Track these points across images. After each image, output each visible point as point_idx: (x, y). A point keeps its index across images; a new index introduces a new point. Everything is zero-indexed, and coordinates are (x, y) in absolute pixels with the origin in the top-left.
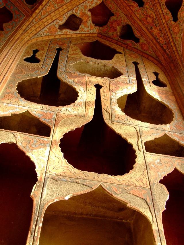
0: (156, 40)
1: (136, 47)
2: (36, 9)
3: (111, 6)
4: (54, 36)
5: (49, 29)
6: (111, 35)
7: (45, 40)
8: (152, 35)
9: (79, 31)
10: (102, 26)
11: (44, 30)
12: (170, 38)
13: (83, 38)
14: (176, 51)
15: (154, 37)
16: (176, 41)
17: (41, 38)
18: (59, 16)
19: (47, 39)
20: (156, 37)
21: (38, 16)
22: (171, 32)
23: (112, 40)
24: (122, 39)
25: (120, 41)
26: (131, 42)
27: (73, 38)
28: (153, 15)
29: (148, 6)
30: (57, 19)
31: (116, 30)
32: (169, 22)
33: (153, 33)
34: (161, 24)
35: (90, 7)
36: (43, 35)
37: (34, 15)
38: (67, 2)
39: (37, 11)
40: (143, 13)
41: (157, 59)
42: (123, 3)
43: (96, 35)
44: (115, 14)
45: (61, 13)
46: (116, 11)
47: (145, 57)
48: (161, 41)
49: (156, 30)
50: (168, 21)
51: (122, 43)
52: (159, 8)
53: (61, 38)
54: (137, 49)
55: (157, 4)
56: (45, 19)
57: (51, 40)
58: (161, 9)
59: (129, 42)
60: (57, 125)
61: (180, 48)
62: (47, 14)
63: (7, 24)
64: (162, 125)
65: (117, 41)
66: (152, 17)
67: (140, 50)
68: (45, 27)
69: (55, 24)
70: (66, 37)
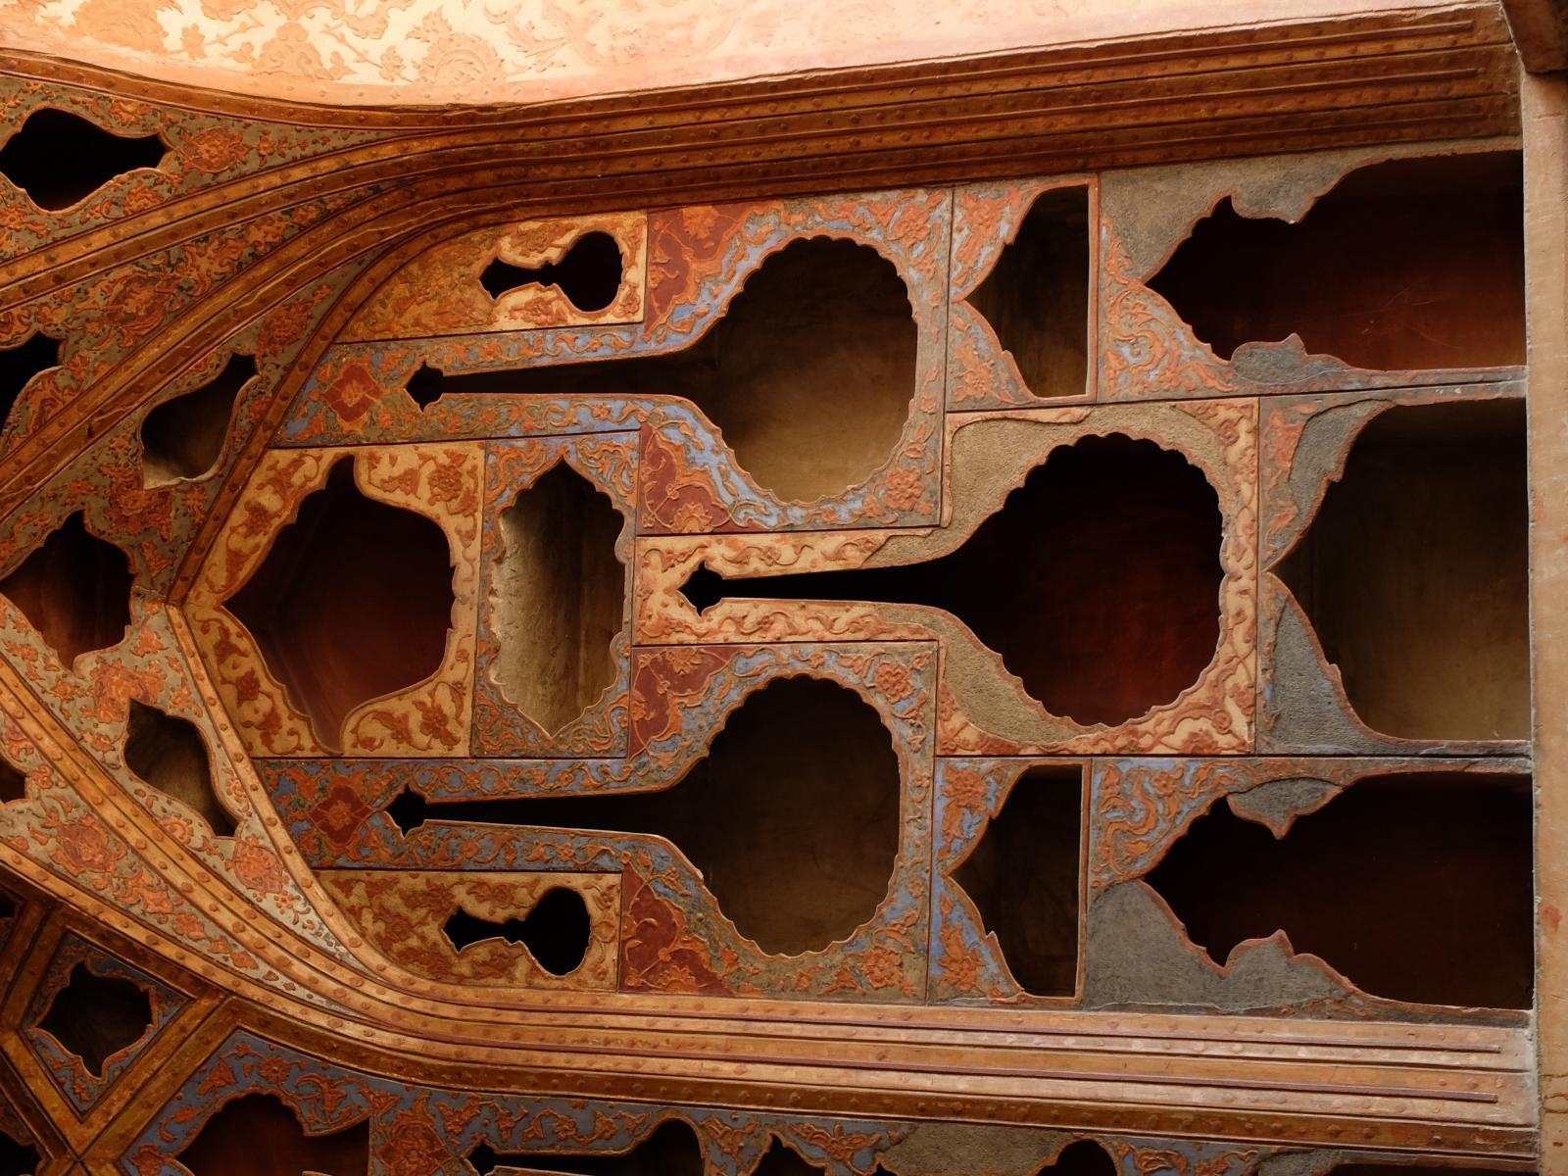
0: (257, 259)
1: (275, 379)
2: (178, 970)
3: (30, 532)
4: (287, 857)
5: (262, 884)
6: (186, 521)
7: (335, 901)
8: (225, 282)
9: (200, 716)
10: (130, 579)
11: (282, 913)
12: (262, 183)
13: (229, 692)
14: (346, 157)
15: (240, 269)
16: (283, 155)
17: (330, 921)
18: (168, 840)
19: (317, 888)
20: (240, 264)
21: (218, 957)
22: (222, 178)
23: (216, 519)
24: (221, 457)
25: (226, 470)
26: (245, 407)
27: (248, 747)
28: (114, 282)
29: (60, 316)
30: (187, 851)
31: (164, 494)
32: (163, 190)
33: (213, 281)
34: (173, 235)
35: (54, 661)
36: (312, 916)
37: (221, 978)
38: (82, 802)
39: (195, 964)
40: (94, 341)
41: (368, 258)
42: (19, 463)
43: (174, 612)
44: (77, 507)
45: (149, 832)
46: (61, 500)
47: (347, 322)
48: (266, 233)
49: (204, 264)
50: (157, 196)
51: (240, 455)
52: (79, 248)
53: (279, 813)
54: (289, 369)
55: (59, 261)
56: (217, 916)
57: (316, 870)
58: (83, 235)
59: (243, 414)
60: (1010, 746)
61: (329, 132)
62: (186, 907)
63: (305, 1113)
64: (914, 302)
65: (224, 483)
66: (126, 286)
67: (300, 354)
68: (265, 914)
69: (221, 855)
70: (260, 787)
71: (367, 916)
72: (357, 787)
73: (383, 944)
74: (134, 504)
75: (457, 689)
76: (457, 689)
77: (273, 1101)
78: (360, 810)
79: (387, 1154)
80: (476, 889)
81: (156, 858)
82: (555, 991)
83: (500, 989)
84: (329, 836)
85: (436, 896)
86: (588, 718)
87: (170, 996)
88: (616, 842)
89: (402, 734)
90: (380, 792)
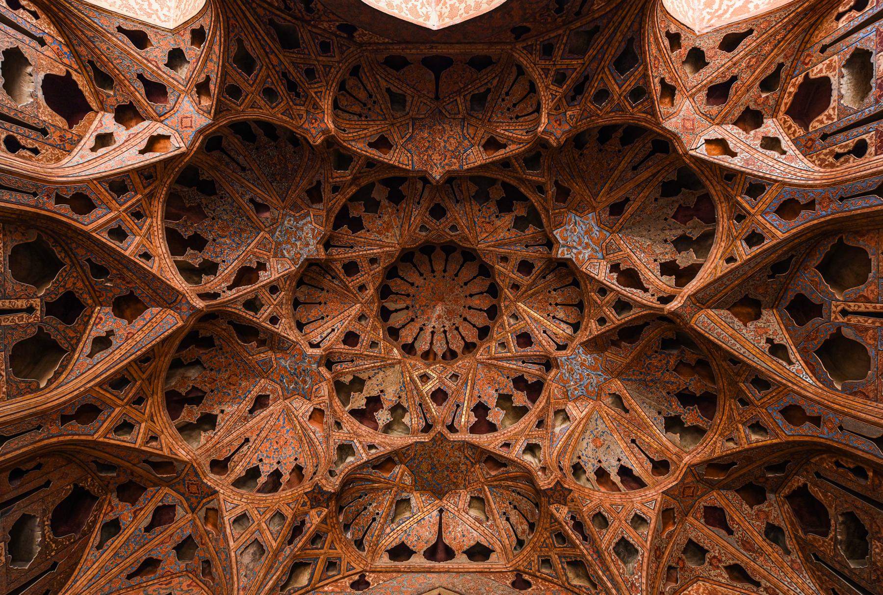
2: (770, 179)
37: (780, 179)
39: (774, 177)
63: (800, 200)
71: (816, 162)
72: (813, 137)
73: (820, 166)
74: (760, 101)
75: (834, 108)
76: (834, 108)
77: (793, 199)
78: (813, 141)
79: (820, 204)
80: (840, 147)
81: (766, 161)
82: (860, 161)
83: (847, 165)
84: (806, 148)
85: (831, 152)
86: (866, 100)
87: (770, 184)
88: (874, 125)
89: (821, 122)
90: (818, 135)
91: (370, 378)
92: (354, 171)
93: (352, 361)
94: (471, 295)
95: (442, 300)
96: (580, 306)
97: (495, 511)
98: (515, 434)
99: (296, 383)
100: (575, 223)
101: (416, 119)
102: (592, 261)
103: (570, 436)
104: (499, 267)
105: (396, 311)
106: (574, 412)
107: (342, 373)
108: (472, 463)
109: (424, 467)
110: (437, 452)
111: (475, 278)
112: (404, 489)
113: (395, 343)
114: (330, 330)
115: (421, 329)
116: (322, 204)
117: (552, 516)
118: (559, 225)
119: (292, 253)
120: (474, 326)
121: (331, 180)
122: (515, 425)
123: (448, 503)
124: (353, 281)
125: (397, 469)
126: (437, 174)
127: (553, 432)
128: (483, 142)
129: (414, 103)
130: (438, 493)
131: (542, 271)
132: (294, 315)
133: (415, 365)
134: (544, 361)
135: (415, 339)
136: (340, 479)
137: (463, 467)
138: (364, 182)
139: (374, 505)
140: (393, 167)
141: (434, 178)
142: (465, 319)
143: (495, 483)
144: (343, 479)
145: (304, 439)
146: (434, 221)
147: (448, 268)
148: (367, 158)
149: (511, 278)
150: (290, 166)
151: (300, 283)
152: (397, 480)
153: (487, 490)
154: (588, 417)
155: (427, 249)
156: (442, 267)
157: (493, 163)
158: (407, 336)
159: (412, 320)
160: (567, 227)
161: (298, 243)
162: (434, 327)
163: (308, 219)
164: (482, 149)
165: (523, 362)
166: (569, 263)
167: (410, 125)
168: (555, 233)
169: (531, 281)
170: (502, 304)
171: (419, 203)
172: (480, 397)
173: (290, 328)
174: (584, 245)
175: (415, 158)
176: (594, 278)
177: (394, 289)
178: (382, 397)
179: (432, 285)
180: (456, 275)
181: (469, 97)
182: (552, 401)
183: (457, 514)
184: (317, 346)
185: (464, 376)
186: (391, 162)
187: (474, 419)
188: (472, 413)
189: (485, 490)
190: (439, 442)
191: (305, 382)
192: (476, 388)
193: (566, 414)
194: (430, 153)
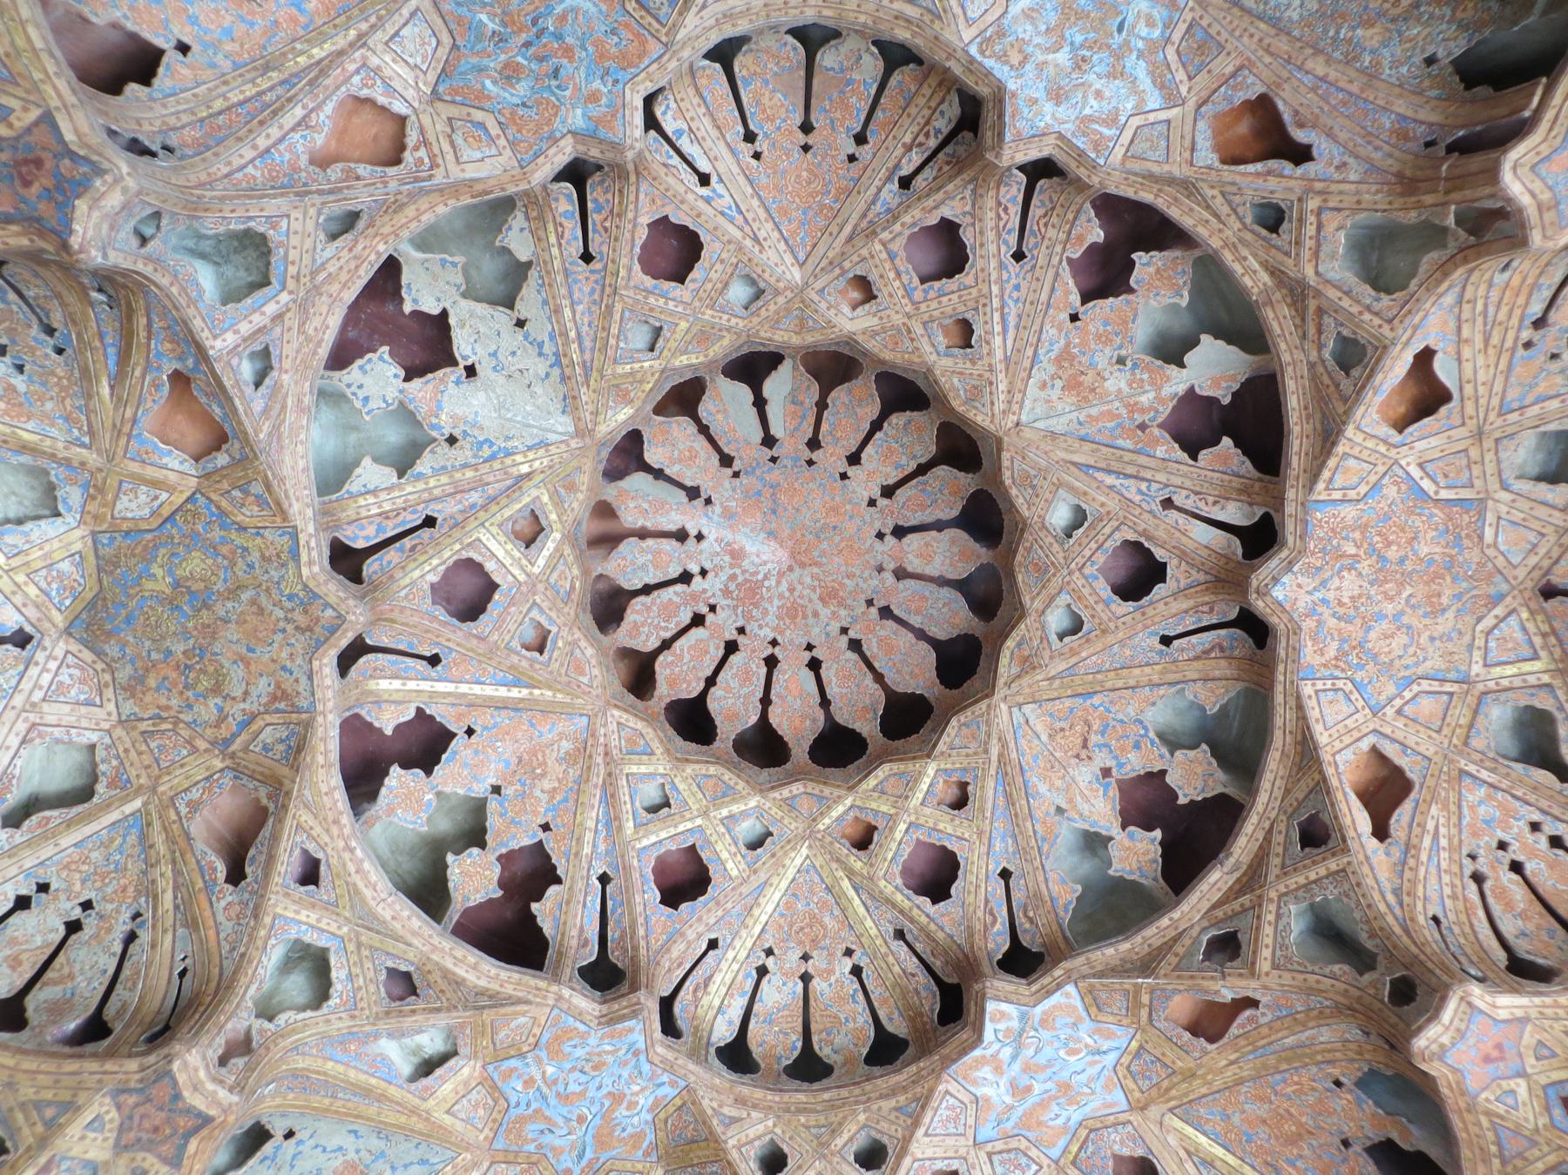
91: (520, 324)
92: (1333, 294)
93: (587, 257)
94: (815, 665)
95: (800, 559)
96: (809, 1067)
97: (47, 851)
98: (354, 891)
99: (500, 39)
100: (1099, 1052)
101: (1481, 514)
102: (971, 1111)
103: (366, 1092)
104: (931, 776)
105: (760, 403)
106: (448, 1087)
107: (541, 218)
108: (227, 742)
109: (195, 564)
110: (261, 611)
111: (879, 678)
112: (95, 490)
113: (650, 407)
114: (704, 166)
115: (693, 493)
116: (1212, 159)
117: (70, 1107)
118: (1094, 1003)
119: (1025, 30)
120: (711, 681)
121: (1313, 204)
122: (384, 884)
123: (57, 661)
124: (892, 256)
125: (176, 466)
126: (1285, 589)
127: (377, 1037)
128: (1390, 750)
129: (1542, 512)
130: (93, 623)
131: (922, 929)
132: (774, 28)
133: (571, 488)
134: (614, 956)
135: (658, 474)
136: (126, 264)
137: (207, 710)
138: (1278, 321)
139: (19, 382)
140: (1328, 437)
141: (1276, 580)
142: (731, 647)
143: (159, 839)
144: (126, 273)
145: (275, 83)
146: (1101, 558)
147: (910, 583)
148: (1383, 349)
149: (892, 820)
150: (1369, 36)
151: (895, 56)
152: (134, 467)
153: (129, 808)
154: (435, 1135)
155: (986, 518)
156: (914, 565)
157: (1322, 787)
158: (673, 443)
159: (726, 461)
160: (1087, 1025)
161: (1063, 57)
162: (700, 537)
163: (1154, 100)
164: (1365, 745)
165: (604, 879)
166: (965, 1035)
167: (1466, 494)
168: (1070, 988)
169: (889, 889)
170: (797, 788)
171: (1168, 503)
172: (470, 732)
173: (728, 16)
174: (1024, 1081)
175: (1349, 512)
176: (916, 1123)
177: (839, 395)
178: (449, 376)
179: (850, 527)
180: (886, 613)
181: (1544, 702)
182: (487, 1016)
183: (18, 700)
184: (651, 123)
185: (542, 675)
186: (1350, 431)
187: (387, 721)
188: (410, 714)
189: (126, 800)
190: (302, 620)
191: (510, 74)
192: (503, 718)
193: (443, 1059)
194: (1365, 566)
